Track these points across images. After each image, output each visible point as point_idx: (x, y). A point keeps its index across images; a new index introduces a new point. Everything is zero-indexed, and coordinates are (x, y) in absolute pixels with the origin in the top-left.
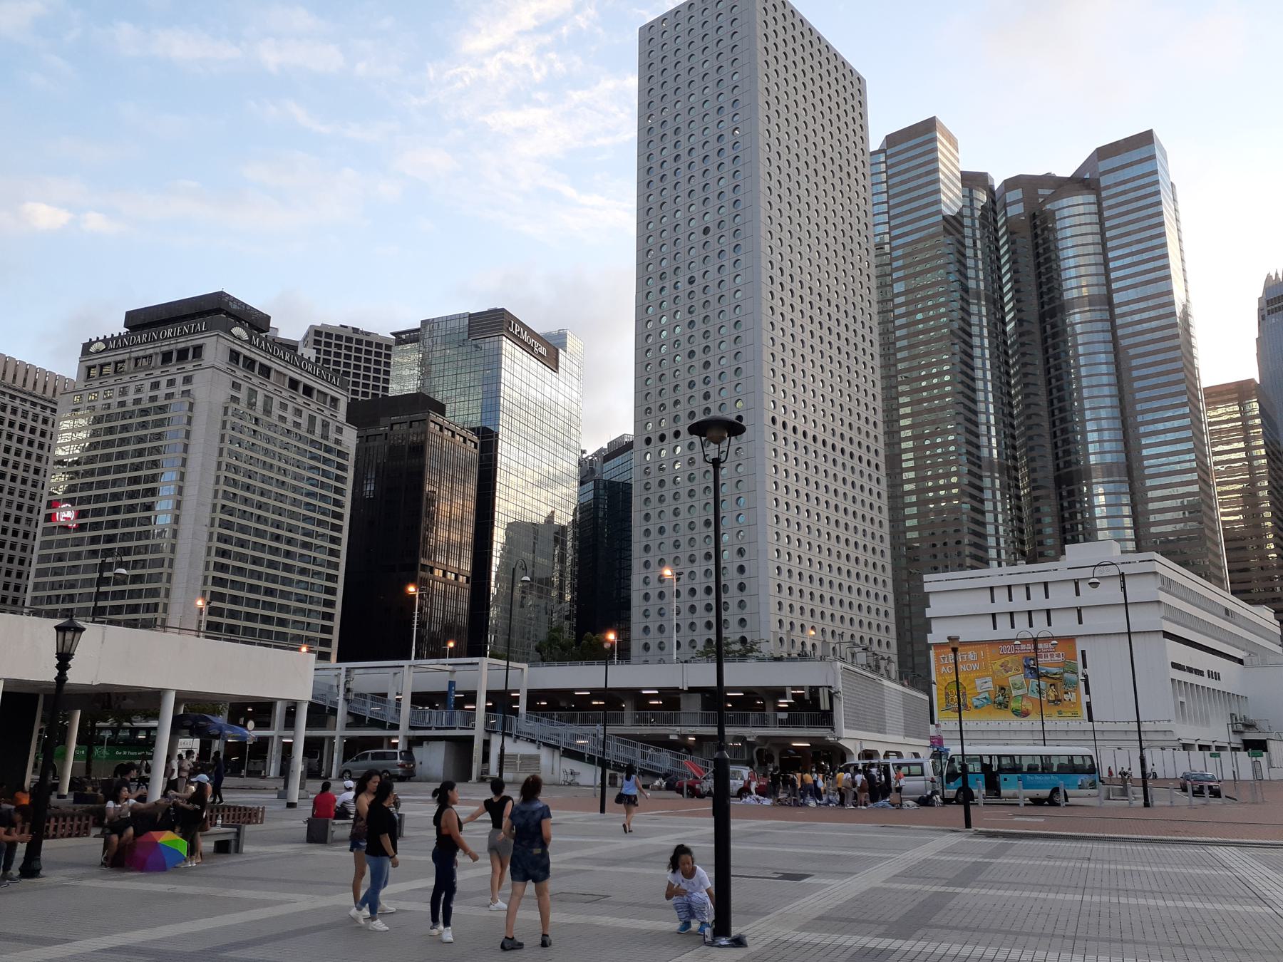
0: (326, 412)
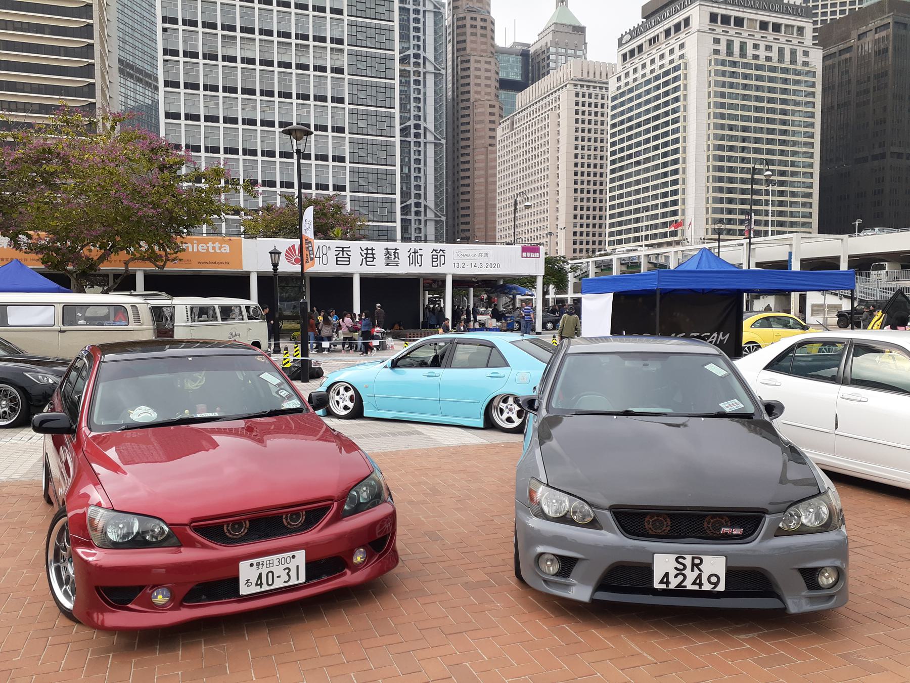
0: (795, 42)
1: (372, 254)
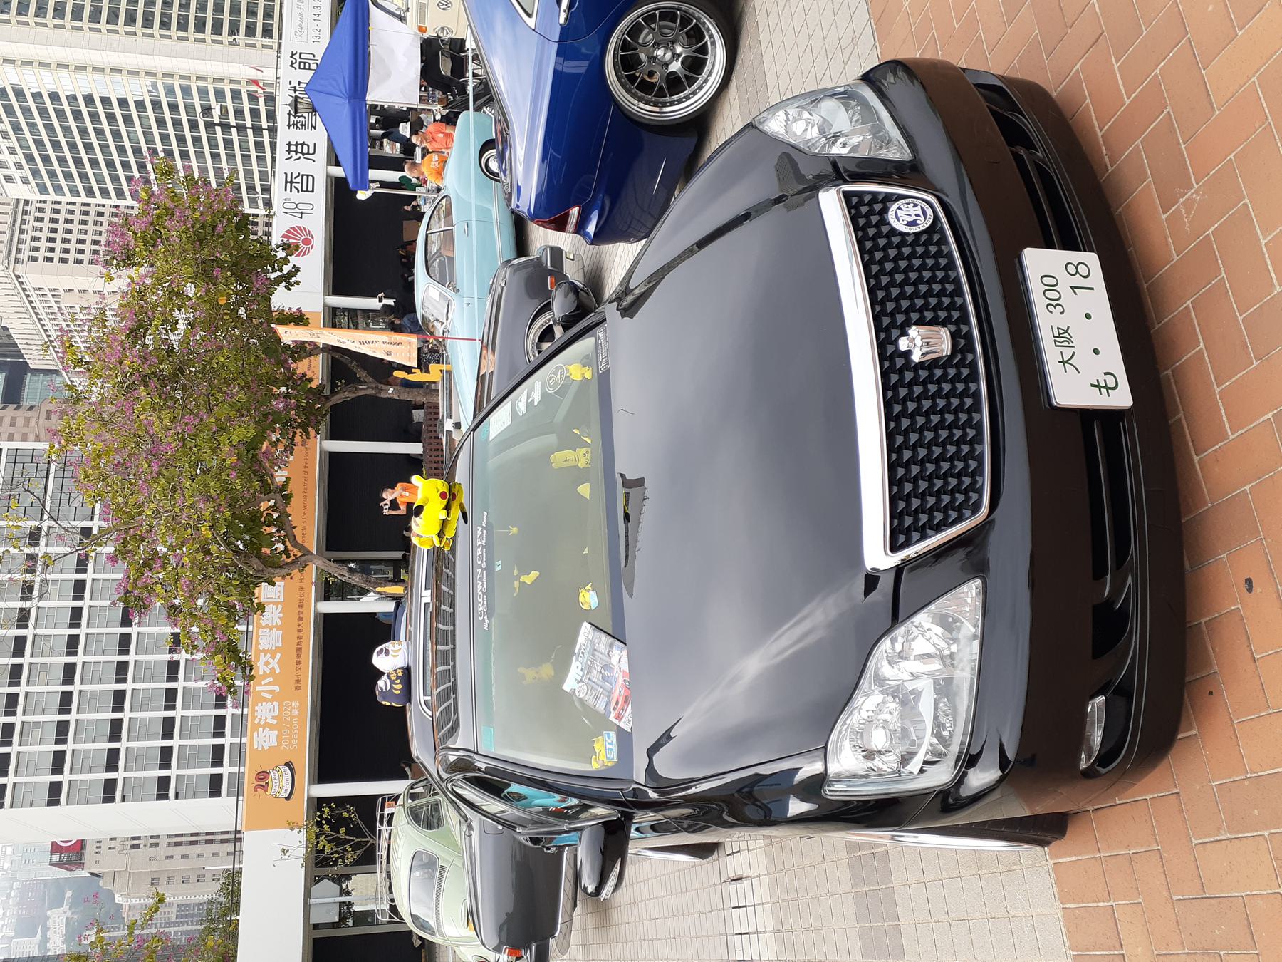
1: (297, 145)
